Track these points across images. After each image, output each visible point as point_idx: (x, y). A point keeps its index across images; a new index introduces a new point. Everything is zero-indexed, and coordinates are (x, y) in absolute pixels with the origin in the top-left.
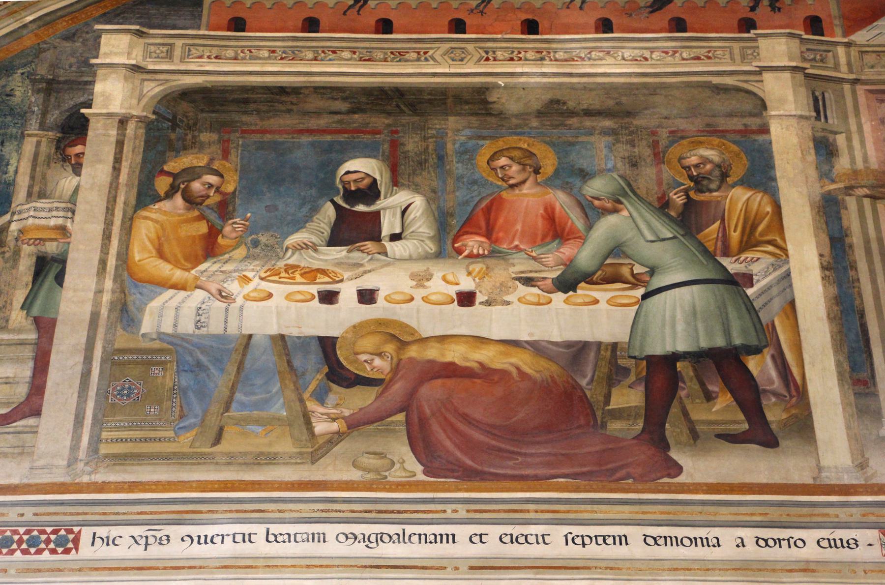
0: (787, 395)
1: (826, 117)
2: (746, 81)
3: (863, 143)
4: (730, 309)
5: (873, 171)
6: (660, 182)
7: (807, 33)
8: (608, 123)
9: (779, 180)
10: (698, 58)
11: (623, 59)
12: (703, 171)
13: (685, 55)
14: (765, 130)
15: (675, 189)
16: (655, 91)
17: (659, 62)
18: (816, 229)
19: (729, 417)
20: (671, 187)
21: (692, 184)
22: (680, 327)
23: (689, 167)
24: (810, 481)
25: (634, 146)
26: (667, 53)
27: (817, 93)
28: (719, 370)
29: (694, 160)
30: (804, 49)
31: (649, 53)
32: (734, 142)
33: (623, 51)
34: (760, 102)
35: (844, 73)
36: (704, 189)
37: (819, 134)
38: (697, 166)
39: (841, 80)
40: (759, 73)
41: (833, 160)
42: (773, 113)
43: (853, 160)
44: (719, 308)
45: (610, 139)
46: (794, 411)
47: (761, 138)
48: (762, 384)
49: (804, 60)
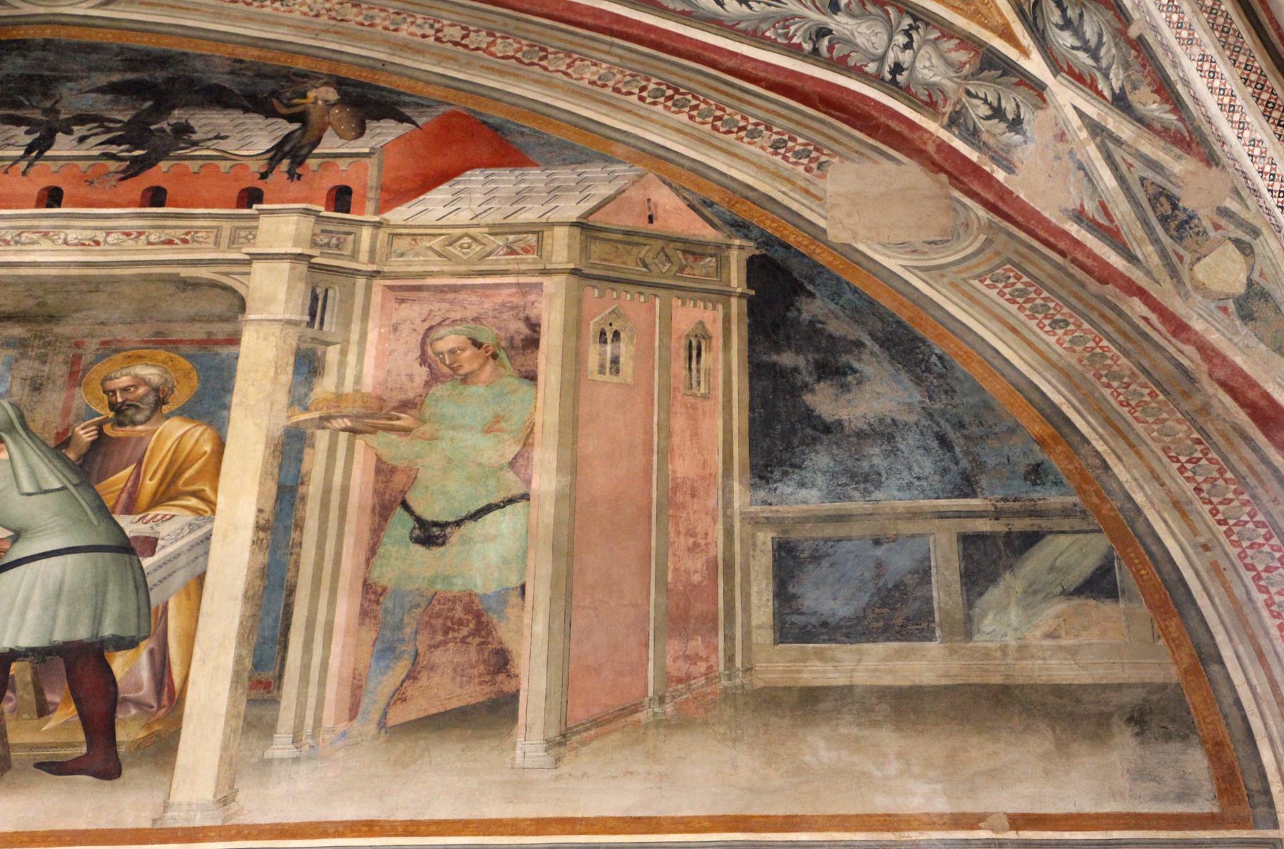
0: (155, 705)
1: (322, 323)
2: (226, 274)
3: (361, 356)
4: (111, 586)
5: (363, 395)
6: (66, 412)
7: (327, 209)
8: (17, 331)
9: (233, 408)
10: (170, 242)
11: (66, 243)
12: (130, 397)
13: (153, 238)
14: (234, 340)
15: (84, 421)
16: (97, 287)
17: (114, 248)
18: (265, 473)
19: (64, 738)
20: (80, 419)
21: (111, 415)
22: (32, 614)
23: (114, 392)
24: (145, 823)
25: (44, 363)
26: (128, 235)
27: (318, 291)
28: (69, 671)
29: (124, 381)
30: (318, 231)
31: (104, 235)
32: (187, 357)
33: (68, 231)
34: (237, 302)
35: (363, 264)
36: (127, 421)
37: (305, 346)
38: (125, 390)
39: (356, 273)
40: (248, 263)
41: (315, 380)
42: (252, 317)
43: (341, 379)
44: (97, 586)
45: (12, 353)
46: (156, 728)
47: (225, 351)
48: (124, 690)
49: (314, 244)
